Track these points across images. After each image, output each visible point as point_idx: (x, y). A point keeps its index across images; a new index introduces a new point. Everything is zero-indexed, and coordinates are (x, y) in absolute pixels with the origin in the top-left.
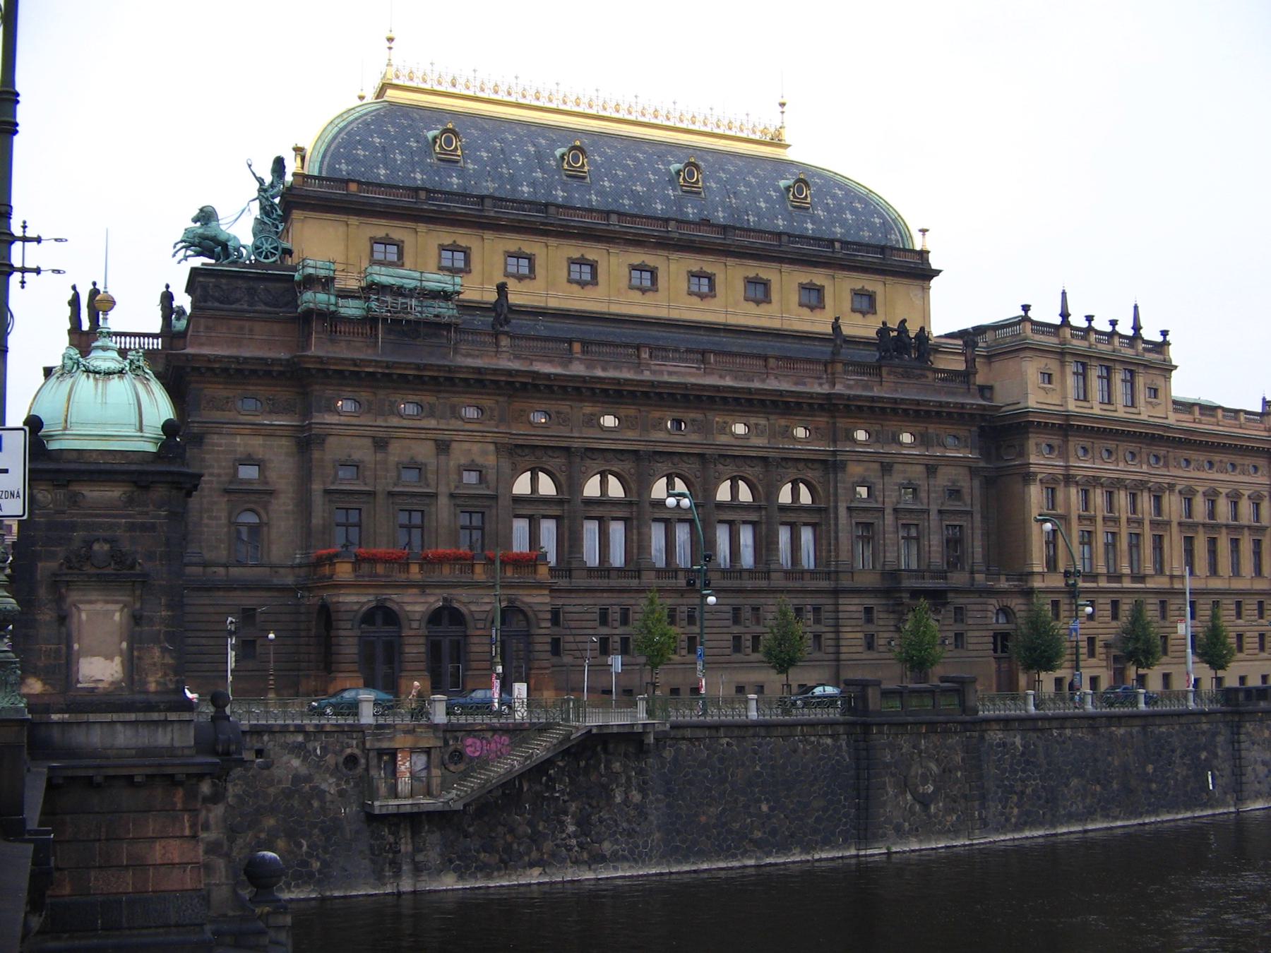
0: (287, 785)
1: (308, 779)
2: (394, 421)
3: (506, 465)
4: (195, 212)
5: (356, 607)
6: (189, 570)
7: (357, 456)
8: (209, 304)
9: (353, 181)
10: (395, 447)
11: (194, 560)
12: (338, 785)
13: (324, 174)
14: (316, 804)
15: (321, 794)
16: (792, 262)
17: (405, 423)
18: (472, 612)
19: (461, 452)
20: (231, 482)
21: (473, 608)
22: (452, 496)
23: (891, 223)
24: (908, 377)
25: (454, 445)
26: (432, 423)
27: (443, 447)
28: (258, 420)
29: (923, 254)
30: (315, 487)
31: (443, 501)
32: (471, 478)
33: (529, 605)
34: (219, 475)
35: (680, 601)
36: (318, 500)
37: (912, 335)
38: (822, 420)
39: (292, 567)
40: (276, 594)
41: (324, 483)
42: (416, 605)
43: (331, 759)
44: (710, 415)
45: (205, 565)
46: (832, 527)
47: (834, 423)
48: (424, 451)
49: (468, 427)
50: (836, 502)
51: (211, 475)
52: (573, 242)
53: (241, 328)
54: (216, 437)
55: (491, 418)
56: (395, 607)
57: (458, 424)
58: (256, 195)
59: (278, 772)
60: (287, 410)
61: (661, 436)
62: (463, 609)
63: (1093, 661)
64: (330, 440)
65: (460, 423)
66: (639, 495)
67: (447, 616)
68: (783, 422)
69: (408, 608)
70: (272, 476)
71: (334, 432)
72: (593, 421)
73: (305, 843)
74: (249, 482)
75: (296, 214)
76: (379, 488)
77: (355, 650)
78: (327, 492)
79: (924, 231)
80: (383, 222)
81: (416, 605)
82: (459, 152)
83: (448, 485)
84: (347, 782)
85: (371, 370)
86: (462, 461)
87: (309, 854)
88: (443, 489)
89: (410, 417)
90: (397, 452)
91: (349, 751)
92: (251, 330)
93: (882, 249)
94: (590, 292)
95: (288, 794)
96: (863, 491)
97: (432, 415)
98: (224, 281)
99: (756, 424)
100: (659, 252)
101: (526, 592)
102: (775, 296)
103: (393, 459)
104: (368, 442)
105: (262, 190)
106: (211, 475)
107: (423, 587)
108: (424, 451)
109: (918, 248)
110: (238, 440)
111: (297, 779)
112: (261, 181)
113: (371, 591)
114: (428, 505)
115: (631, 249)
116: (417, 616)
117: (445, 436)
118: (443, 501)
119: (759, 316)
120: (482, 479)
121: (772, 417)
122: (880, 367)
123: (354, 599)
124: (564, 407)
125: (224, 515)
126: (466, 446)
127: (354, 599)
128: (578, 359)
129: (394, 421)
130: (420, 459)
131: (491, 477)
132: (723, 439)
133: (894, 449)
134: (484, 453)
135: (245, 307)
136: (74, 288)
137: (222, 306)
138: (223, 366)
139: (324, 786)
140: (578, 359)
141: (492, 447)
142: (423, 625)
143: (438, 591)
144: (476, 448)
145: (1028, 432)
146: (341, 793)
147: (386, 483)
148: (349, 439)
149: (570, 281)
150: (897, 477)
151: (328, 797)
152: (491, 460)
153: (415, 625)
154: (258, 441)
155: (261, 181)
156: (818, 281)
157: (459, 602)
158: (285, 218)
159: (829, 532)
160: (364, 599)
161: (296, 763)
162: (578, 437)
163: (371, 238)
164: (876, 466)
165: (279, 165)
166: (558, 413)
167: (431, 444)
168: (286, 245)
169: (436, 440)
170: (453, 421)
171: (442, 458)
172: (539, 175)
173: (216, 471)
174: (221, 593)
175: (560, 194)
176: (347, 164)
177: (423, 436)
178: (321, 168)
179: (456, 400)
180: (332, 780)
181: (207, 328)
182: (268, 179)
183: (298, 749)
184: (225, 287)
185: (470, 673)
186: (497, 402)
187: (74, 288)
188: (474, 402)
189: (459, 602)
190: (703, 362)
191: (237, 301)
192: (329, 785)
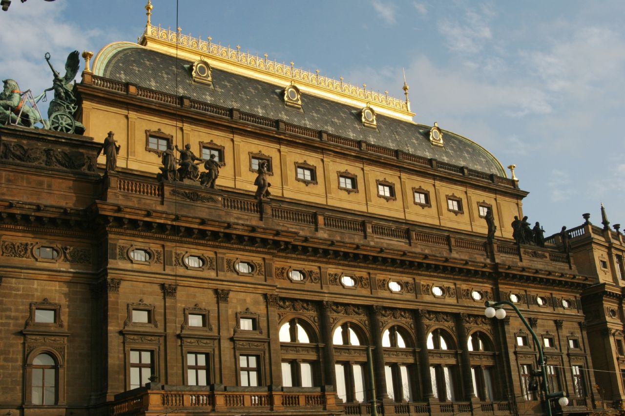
2: (181, 271)
7: (148, 300)
8: (11, 160)
9: (133, 85)
10: (180, 293)
13: (108, 77)
16: (442, 179)
20: (27, 324)
23: (492, 161)
25: (231, 295)
27: (221, 296)
29: (513, 182)
34: (16, 318)
37: (532, 227)
44: (418, 278)
47: (497, 289)
48: (207, 299)
49: (242, 279)
51: (8, 317)
52: (298, 151)
53: (41, 183)
58: (51, 85)
61: (386, 294)
64: (123, 285)
65: (235, 275)
68: (464, 286)
71: (128, 277)
72: (336, 280)
74: (46, 325)
75: (86, 104)
80: (156, 119)
82: (210, 79)
85: (162, 221)
86: (239, 310)
92: (49, 186)
93: (491, 177)
94: (311, 188)
96: (520, 342)
98: (25, 142)
100: (357, 164)
103: (180, 306)
104: (157, 288)
105: (56, 78)
106: (8, 317)
109: (509, 177)
112: (56, 76)
115: (338, 160)
117: (225, 286)
118: (226, 345)
119: (425, 216)
121: (458, 282)
125: (20, 357)
126: (242, 296)
128: (322, 229)
130: (203, 305)
131: (263, 324)
132: (427, 298)
133: (534, 308)
134: (256, 303)
135: (43, 165)
137: (23, 163)
138: (24, 212)
140: (322, 229)
141: (261, 298)
144: (249, 298)
149: (298, 180)
152: (261, 309)
155: (56, 76)
158: (79, 103)
163: (146, 131)
165: (73, 61)
167: (211, 292)
168: (78, 124)
171: (222, 305)
172: (268, 102)
173: (13, 314)
175: (284, 117)
176: (125, 74)
177: (205, 285)
178: (105, 70)
181: (9, 181)
182: (62, 73)
184: (26, 147)
186: (264, 259)
188: (245, 258)
191: (37, 159)
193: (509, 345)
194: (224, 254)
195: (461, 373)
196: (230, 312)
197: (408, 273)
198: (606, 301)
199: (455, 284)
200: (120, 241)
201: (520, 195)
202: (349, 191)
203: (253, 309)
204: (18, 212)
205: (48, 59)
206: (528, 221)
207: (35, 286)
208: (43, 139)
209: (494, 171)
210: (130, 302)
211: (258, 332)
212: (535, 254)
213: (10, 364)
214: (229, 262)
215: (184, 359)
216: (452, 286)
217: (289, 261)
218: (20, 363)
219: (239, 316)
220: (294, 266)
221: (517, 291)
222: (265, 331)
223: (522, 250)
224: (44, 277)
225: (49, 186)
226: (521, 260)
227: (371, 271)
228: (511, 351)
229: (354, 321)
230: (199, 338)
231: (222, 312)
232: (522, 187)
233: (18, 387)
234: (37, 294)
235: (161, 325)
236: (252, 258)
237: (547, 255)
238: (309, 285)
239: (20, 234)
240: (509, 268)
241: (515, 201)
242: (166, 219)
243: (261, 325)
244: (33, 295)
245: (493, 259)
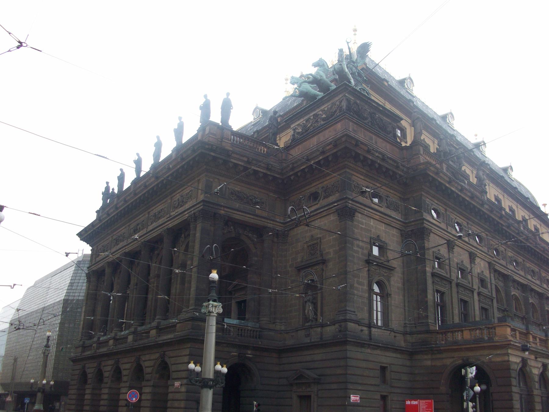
4: (316, 60)
6: (351, 325)
11: (353, 317)
22: (479, 294)
28: (382, 210)
30: (427, 269)
34: (362, 248)
39: (405, 334)
40: (399, 356)
45: (357, 322)
54: (360, 215)
60: (396, 209)
70: (391, 255)
78: (433, 275)
79: (545, 205)
92: (376, 143)
106: (358, 246)
110: (372, 222)
117: (473, 250)
125: (366, 282)
136: (205, 96)
138: (374, 159)
141: (487, 265)
148: (438, 237)
154: (382, 227)
166: (502, 252)
171: (473, 265)
174: (369, 351)
177: (465, 247)
187: (205, 96)
200: (428, 199)
204: (371, 158)
205: (348, 43)
207: (372, 224)
208: (370, 103)
213: (360, 287)
218: (366, 287)
224: (377, 217)
225: (376, 143)
229: (517, 294)
233: (365, 308)
234: (373, 230)
239: (362, 177)
242: (456, 188)
244: (371, 231)
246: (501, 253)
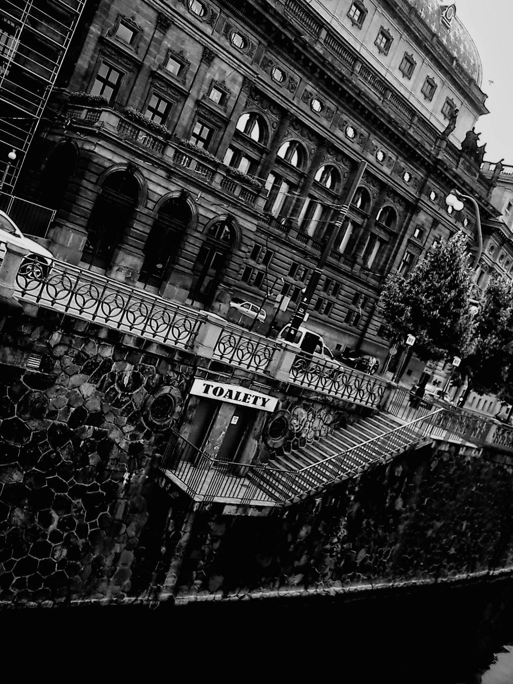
0: (62, 421)
1: (97, 418)
3: (244, 98)
5: (107, 164)
12: (134, 437)
14: (93, 459)
15: (104, 445)
17: (189, 16)
18: (198, 214)
19: (220, 70)
21: (201, 211)
22: (198, 103)
23: (476, 68)
24: (469, 171)
25: (216, 60)
26: (208, 30)
27: (208, 57)
31: (190, 104)
32: (215, 96)
33: (241, 228)
35: (302, 260)
36: (90, 45)
38: (420, 175)
41: (102, 31)
42: (158, 187)
43: (139, 396)
44: (372, 135)
46: (395, 249)
47: (426, 181)
48: (193, 52)
50: (405, 233)
55: (250, 54)
56: (141, 181)
57: (227, 44)
59: (56, 399)
61: (341, 135)
62: (193, 208)
63: (442, 372)
65: (228, 44)
66: (310, 172)
67: (176, 210)
68: (403, 164)
69: (151, 186)
72: (307, 98)
73: (55, 516)
76: (146, 63)
77: (89, 206)
81: (158, 187)
83: (199, 92)
84: (147, 436)
86: (216, 78)
87: (55, 536)
88: (193, 93)
89: (193, 14)
90: (171, 39)
91: (166, 390)
93: (471, 80)
95: (58, 436)
97: (210, 23)
99: (390, 158)
101: (243, 215)
102: (413, 77)
103: (167, 44)
104: (153, 15)
107: (171, 174)
108: (193, 52)
111: (81, 416)
113: (127, 155)
114: (178, 101)
116: (156, 198)
117: (214, 48)
118: (190, 104)
119: (401, 85)
120: (223, 101)
121: (400, 158)
122: (460, 156)
123: (109, 155)
124: (297, 76)
126: (224, 66)
127: (109, 155)
129: (181, 9)
130: (187, 56)
131: (231, 104)
139: (114, 435)
141: (240, 79)
142: (157, 208)
143: (180, 183)
144: (229, 71)
145: (491, 235)
146: (136, 450)
147: (152, 62)
150: (436, 233)
151: (115, 453)
152: (235, 89)
153: (150, 205)
156: (437, 81)
157: (192, 200)
159: (391, 250)
160: (117, 160)
161: (88, 389)
162: (297, 106)
164: (431, 219)
166: (292, 79)
167: (201, 49)
169: (205, 48)
170: (223, 38)
171: (204, 66)
179: (232, 21)
180: (129, 428)
183: (96, 370)
185: (177, 267)
186: (260, 43)
189: (192, 200)
190: (383, 95)
192: (121, 435)
193: (409, 232)
194: (228, 16)
195: (360, 234)
196: (208, 76)
197: (368, 127)
198: (494, 237)
199: (397, 158)
201: (479, 108)
202: (354, 24)
203: (228, 85)
206: (479, 137)
209: (475, 77)
210: (123, 13)
211: (223, 108)
212: (469, 170)
214: (228, 27)
215: (148, 97)
216: (394, 159)
217: (279, 57)
219: (214, 84)
220: (281, 65)
221: (438, 191)
222: (229, 110)
223: (462, 160)
226: (457, 167)
227: (340, 108)
228: (407, 237)
229: (303, 144)
230: (169, 85)
231: (201, 73)
232: (487, 104)
235: (142, 51)
236: (250, 36)
237: (478, 175)
238: (285, 92)
240: (446, 170)
241: (475, 114)
243: (229, 103)
245: (438, 154)
246: (287, 79)
